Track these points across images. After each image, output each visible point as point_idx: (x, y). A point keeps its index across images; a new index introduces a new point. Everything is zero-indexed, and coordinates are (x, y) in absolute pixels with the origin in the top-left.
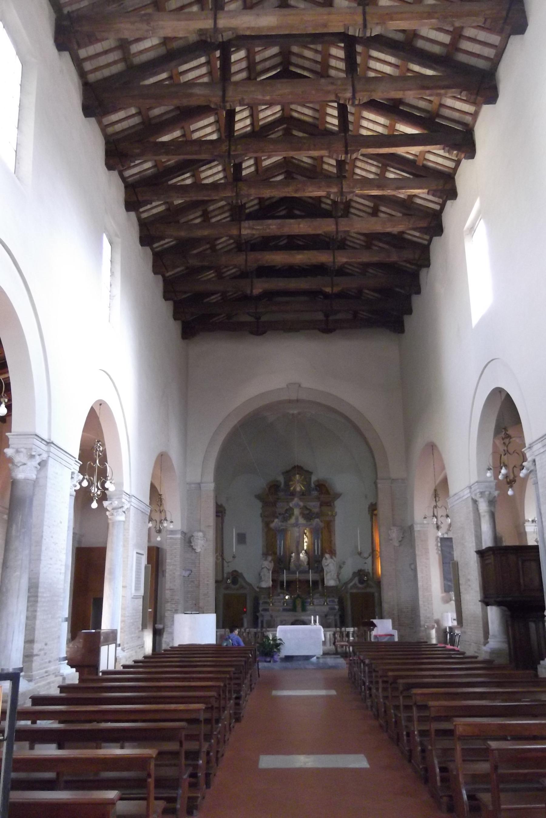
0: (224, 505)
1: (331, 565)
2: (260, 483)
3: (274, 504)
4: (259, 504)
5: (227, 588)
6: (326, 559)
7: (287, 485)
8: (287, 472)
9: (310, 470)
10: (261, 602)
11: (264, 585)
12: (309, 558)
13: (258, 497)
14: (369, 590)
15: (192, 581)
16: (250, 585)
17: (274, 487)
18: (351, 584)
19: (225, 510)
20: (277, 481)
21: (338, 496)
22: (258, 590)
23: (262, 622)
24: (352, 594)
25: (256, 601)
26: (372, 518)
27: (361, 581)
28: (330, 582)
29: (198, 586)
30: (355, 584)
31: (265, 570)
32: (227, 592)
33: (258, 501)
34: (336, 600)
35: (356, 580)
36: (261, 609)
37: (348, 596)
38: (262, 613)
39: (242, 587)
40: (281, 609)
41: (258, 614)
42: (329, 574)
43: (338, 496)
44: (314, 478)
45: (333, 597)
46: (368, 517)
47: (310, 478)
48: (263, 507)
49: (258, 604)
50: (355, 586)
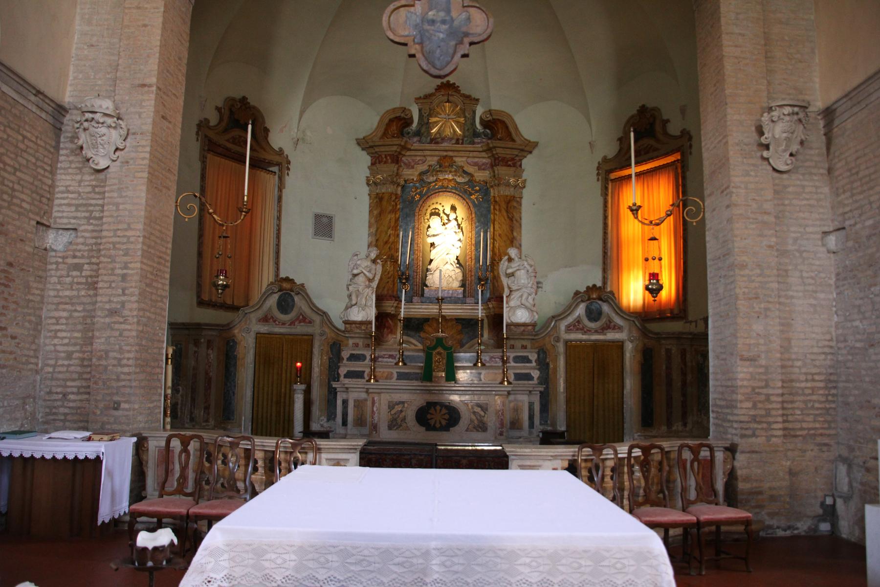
0: (286, 152)
1: (521, 274)
2: (369, 121)
3: (396, 159)
4: (365, 159)
5: (265, 319)
6: (510, 260)
7: (425, 124)
8: (427, 97)
9: (475, 95)
10: (345, 354)
11: (357, 315)
12: (464, 275)
13: (365, 144)
14: (611, 336)
15: (78, 267)
16: (324, 314)
17: (398, 123)
18: (570, 319)
19: (289, 162)
20: (404, 110)
21: (529, 147)
22: (341, 327)
23: (345, 402)
24: (566, 342)
25: (335, 349)
26: (605, 194)
27: (593, 315)
28: (517, 313)
29: (93, 286)
30: (579, 321)
31: (361, 279)
32: (264, 329)
33: (364, 153)
34: (533, 357)
35: (581, 310)
36: (343, 371)
37: (561, 348)
38: (347, 381)
39: (303, 319)
40: (395, 371)
41: (335, 385)
42: (515, 295)
43: (529, 147)
44: (480, 111)
45: (524, 347)
46: (598, 186)
47: (474, 112)
48: (373, 164)
49: (340, 359)
50: (576, 326)
